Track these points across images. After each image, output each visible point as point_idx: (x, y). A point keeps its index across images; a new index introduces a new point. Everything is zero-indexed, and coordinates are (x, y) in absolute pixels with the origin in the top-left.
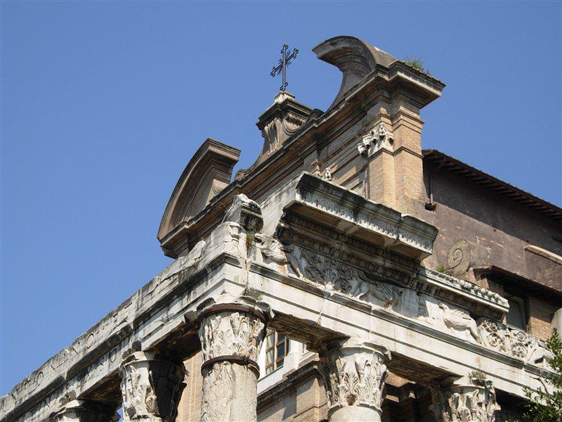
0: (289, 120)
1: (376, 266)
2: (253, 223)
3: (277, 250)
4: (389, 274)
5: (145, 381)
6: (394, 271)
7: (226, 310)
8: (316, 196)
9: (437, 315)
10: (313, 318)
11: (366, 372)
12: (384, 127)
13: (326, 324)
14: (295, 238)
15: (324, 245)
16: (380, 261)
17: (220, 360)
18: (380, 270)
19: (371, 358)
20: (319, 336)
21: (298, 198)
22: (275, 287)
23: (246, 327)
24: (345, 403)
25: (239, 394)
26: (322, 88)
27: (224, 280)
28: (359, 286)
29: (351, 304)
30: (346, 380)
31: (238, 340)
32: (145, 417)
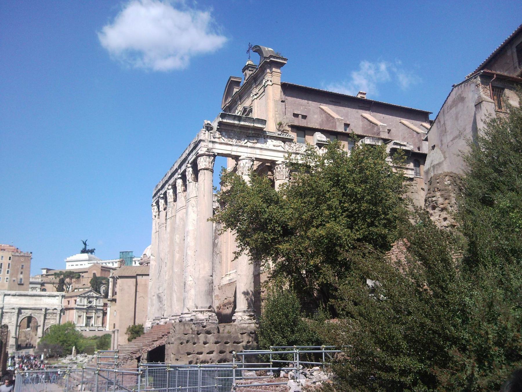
1: (250, 133)
3: (218, 135)
8: (226, 118)
9: (271, 144)
10: (229, 152)
12: (268, 77)
16: (250, 132)
19: (247, 161)
21: (220, 120)
22: (217, 146)
23: (208, 159)
25: (206, 178)
26: (254, 60)
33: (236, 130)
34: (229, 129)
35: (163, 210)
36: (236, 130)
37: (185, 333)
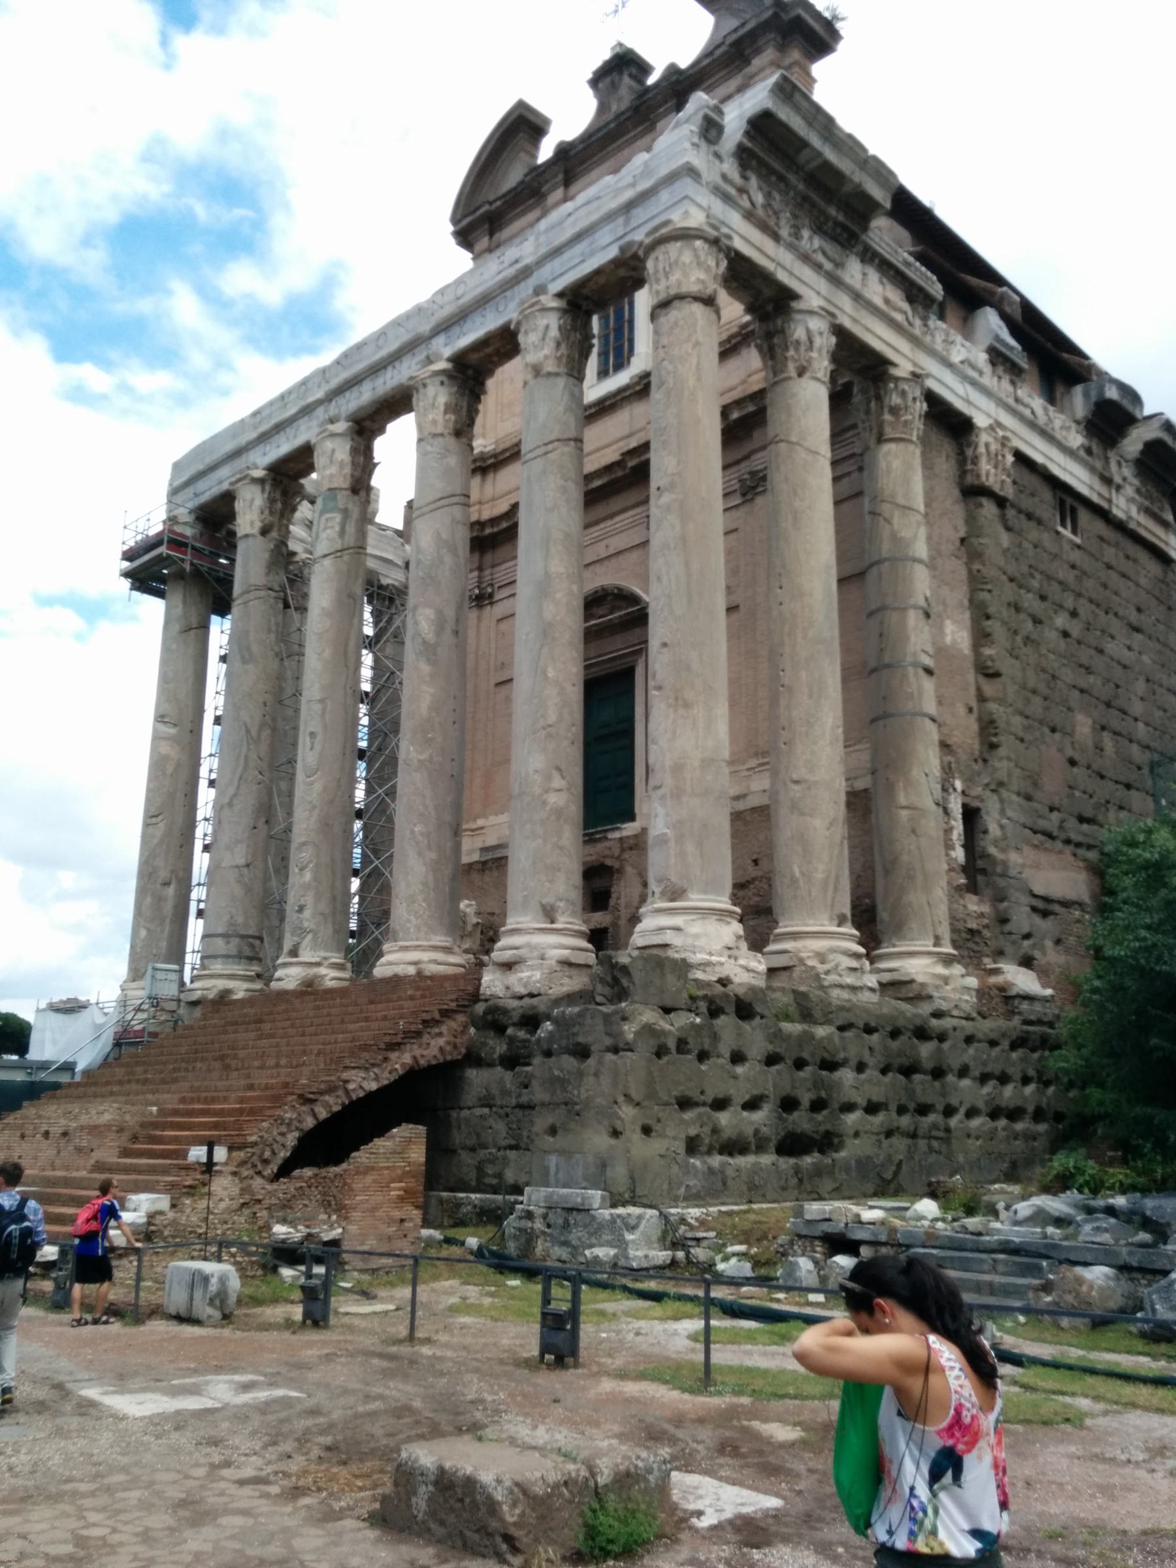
0: (630, 76)
1: (828, 218)
2: (713, 132)
4: (839, 230)
5: (554, 332)
6: (845, 228)
7: (685, 235)
11: (818, 341)
13: (782, 276)
14: (754, 163)
15: (781, 178)
16: (832, 211)
17: (681, 297)
18: (830, 224)
20: (767, 292)
24: (793, 374)
27: (686, 197)
28: (811, 238)
29: (806, 258)
30: (797, 350)
31: (702, 276)
32: (557, 374)
33: (792, 178)
34: (777, 166)
35: (255, 530)
36: (792, 178)
37: (669, 1003)
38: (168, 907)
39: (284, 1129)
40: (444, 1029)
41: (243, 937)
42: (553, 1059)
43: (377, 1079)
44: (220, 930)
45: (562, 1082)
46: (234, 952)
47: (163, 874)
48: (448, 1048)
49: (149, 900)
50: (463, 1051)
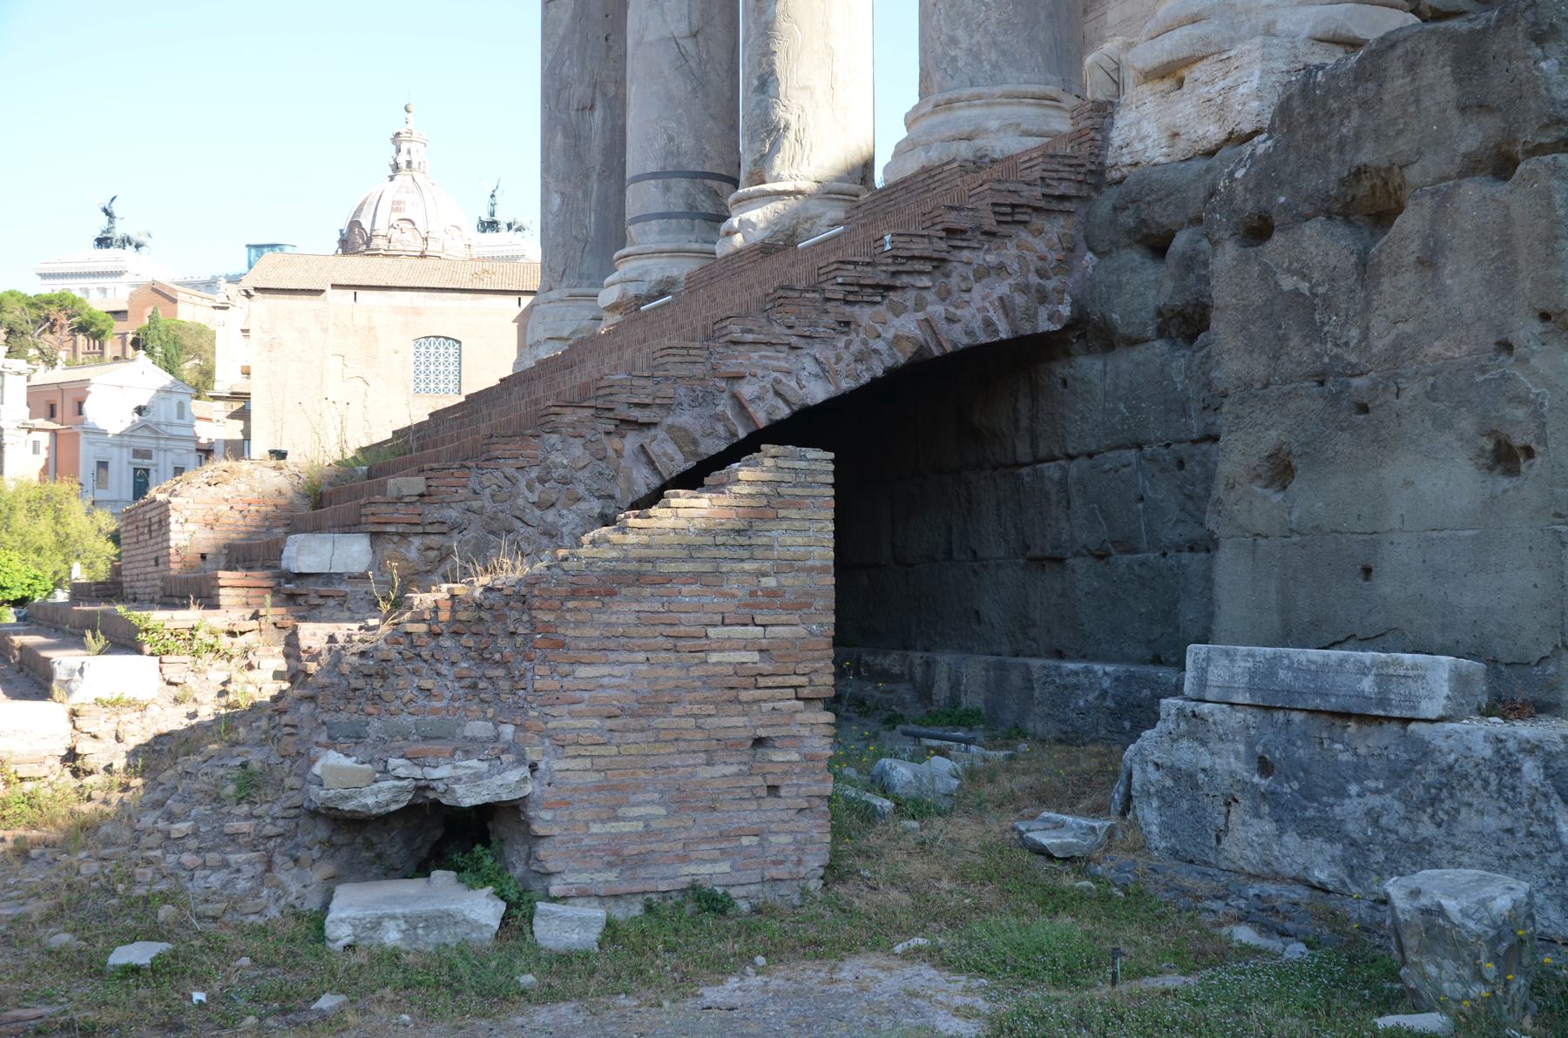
38: (595, 157)
39: (551, 490)
40: (1010, 253)
41: (693, 176)
42: (1278, 238)
43: (824, 373)
44: (652, 167)
45: (1306, 308)
46: (679, 205)
47: (579, 92)
48: (1020, 300)
49: (559, 139)
50: (1066, 310)
